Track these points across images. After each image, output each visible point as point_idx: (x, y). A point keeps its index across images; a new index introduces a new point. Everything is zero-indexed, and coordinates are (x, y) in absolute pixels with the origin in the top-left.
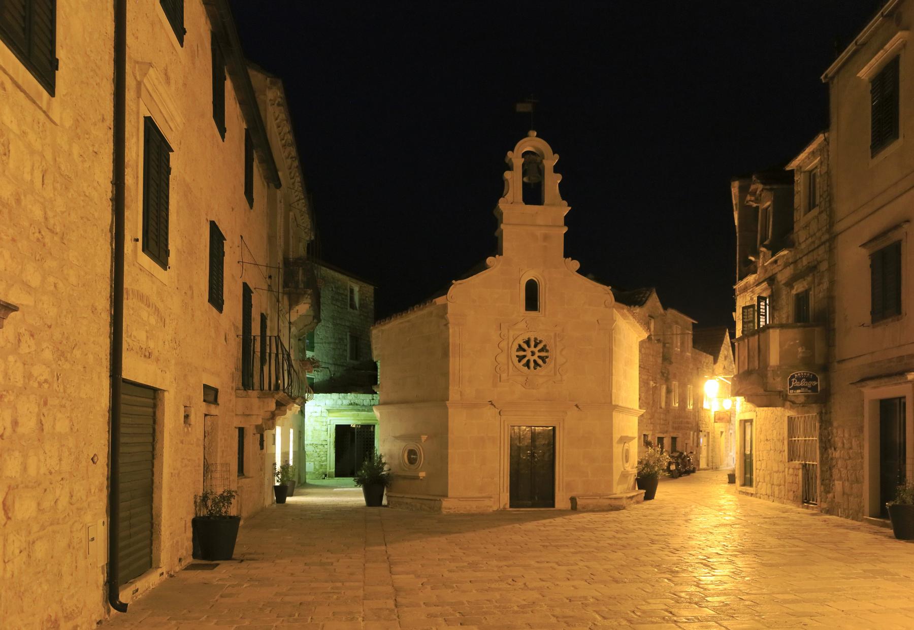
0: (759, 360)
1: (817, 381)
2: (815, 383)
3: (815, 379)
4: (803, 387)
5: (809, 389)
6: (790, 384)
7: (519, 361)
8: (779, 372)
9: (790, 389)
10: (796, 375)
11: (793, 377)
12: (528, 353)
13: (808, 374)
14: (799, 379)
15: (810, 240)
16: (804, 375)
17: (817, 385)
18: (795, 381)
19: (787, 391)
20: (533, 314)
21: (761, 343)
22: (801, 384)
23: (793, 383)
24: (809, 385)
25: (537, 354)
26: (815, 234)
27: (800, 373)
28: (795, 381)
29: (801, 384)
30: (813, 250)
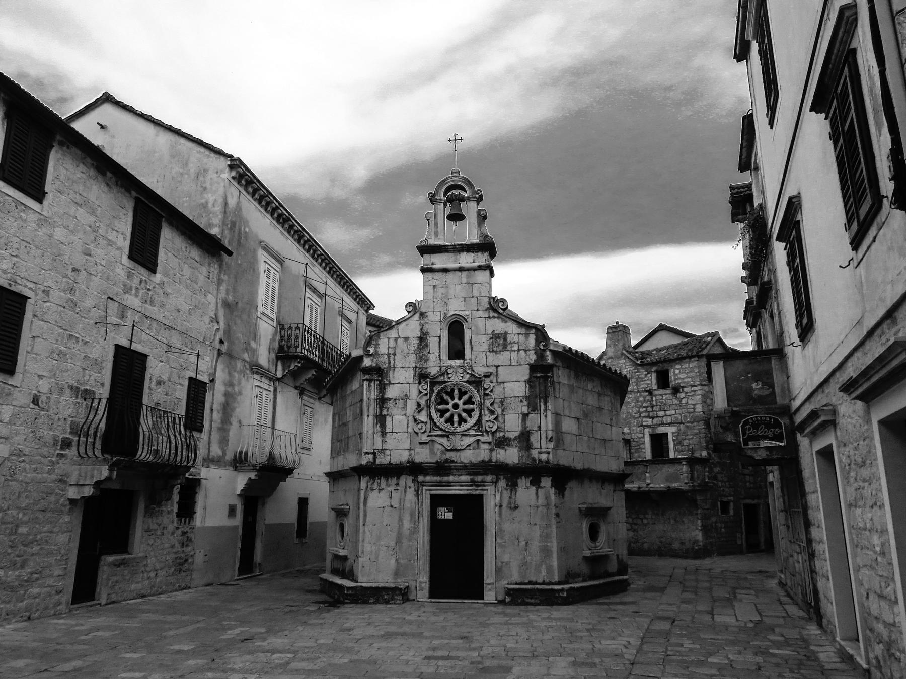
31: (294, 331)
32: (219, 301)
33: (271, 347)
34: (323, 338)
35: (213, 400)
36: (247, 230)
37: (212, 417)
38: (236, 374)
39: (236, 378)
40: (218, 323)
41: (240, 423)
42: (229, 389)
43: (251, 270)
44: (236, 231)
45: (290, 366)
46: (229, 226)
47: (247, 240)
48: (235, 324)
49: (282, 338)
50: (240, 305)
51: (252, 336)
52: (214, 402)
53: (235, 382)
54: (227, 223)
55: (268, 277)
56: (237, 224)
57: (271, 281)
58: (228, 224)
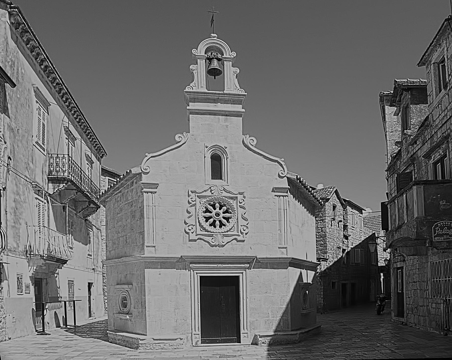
0: (407, 215)
7: (207, 221)
8: (425, 223)
10: (439, 225)
13: (449, 223)
14: (442, 228)
15: (443, 115)
16: (445, 224)
18: (438, 229)
19: (432, 238)
20: (217, 182)
21: (408, 200)
25: (222, 215)
26: (447, 108)
27: (443, 222)
30: (446, 122)
31: (61, 160)
32: (5, 124)
33: (44, 170)
34: (81, 168)
35: (6, 204)
36: (23, 71)
37: (6, 217)
38: (21, 186)
39: (22, 190)
40: (5, 143)
41: (26, 224)
42: (17, 197)
43: (28, 106)
44: (15, 69)
45: (59, 186)
46: (10, 63)
47: (23, 80)
48: (18, 146)
49: (50, 165)
50: (20, 131)
51: (30, 158)
52: (7, 205)
53: (21, 193)
54: (9, 60)
55: (39, 114)
56: (16, 64)
57: (41, 118)
58: (9, 62)
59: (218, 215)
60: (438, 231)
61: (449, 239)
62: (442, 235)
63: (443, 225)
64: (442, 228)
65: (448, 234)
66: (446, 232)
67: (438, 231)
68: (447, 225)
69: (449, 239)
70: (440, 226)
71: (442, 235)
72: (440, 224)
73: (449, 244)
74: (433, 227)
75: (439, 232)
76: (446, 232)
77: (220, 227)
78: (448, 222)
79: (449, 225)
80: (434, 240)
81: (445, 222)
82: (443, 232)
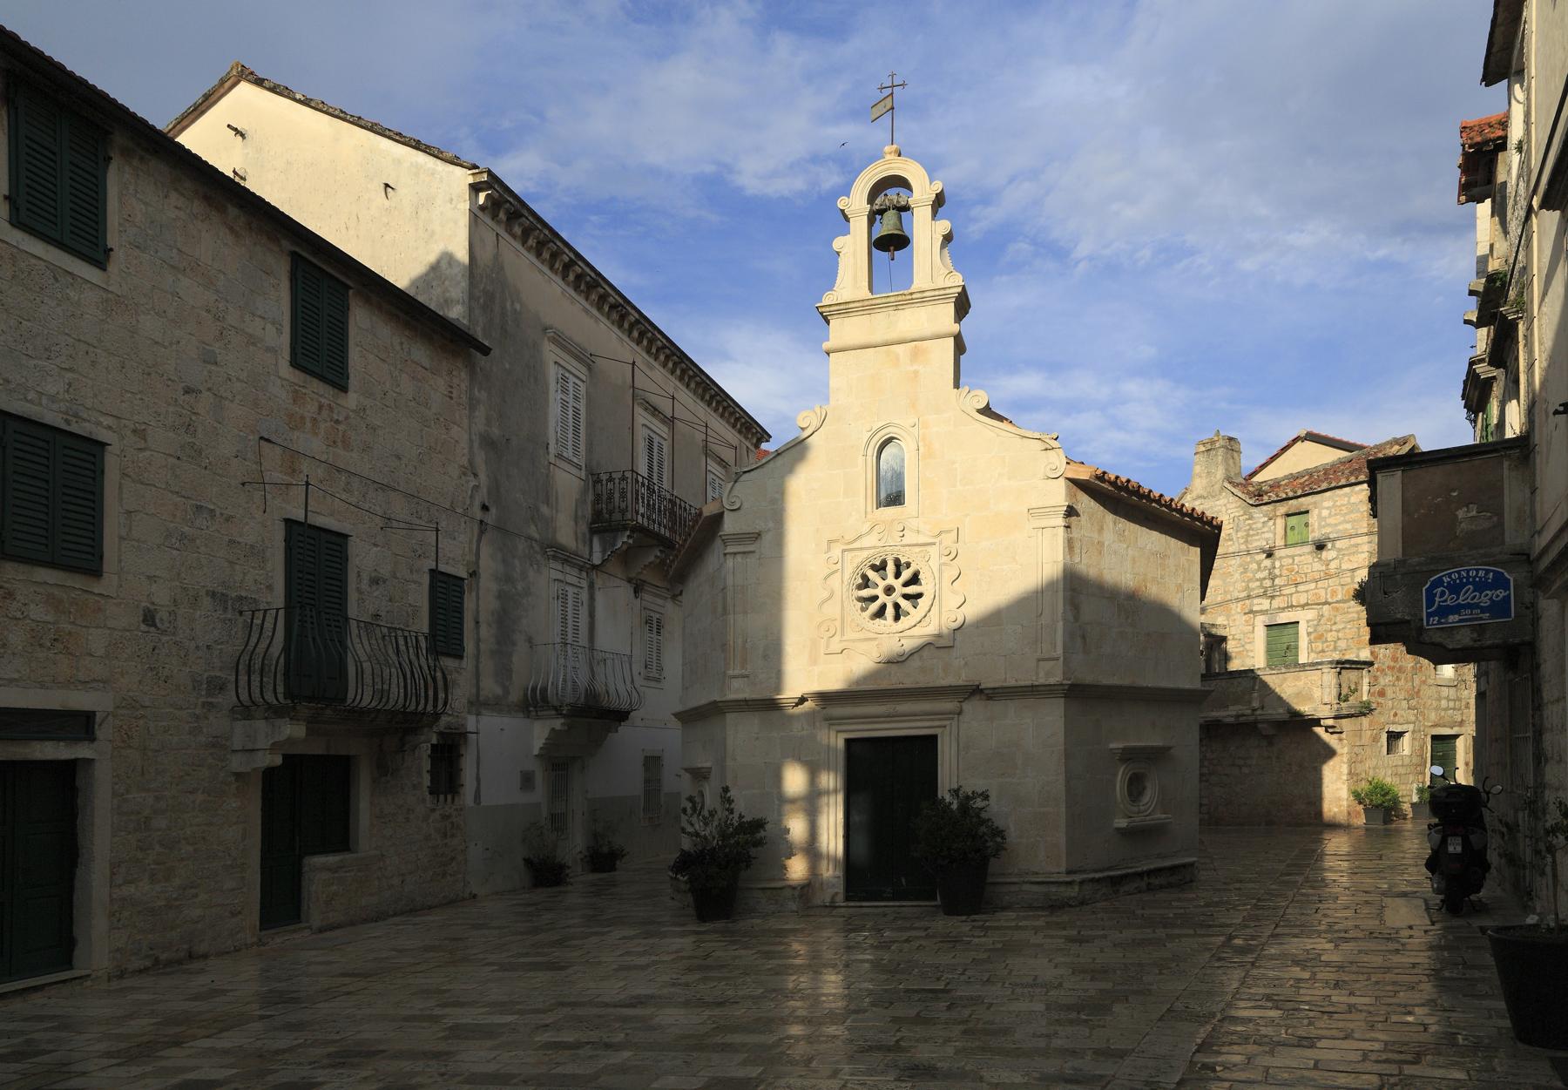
1: (1507, 588)
2: (1501, 593)
3: (1500, 582)
4: (1469, 606)
5: (1483, 610)
6: (1430, 602)
9: (1429, 615)
10: (1446, 580)
11: (1439, 582)
12: (900, 590)
13: (1481, 574)
17: (1510, 594)
18: (1443, 594)
22: (1460, 601)
23: (1437, 599)
24: (1484, 599)
27: (1459, 572)
28: (1443, 594)
29: (1460, 601)
59: (889, 590)
60: (1440, 598)
61: (1481, 619)
62: (1456, 609)
63: (1461, 579)
64: (1455, 588)
65: (1477, 606)
66: (1469, 600)
67: (1440, 598)
68: (1474, 578)
69: (1481, 619)
70: (1448, 583)
71: (1456, 609)
72: (1450, 577)
73: (1479, 636)
74: (1424, 589)
75: (1446, 601)
76: (1469, 600)
77: (897, 618)
78: (1477, 570)
79: (1480, 578)
80: (1428, 625)
81: (1468, 571)
82: (1458, 599)
